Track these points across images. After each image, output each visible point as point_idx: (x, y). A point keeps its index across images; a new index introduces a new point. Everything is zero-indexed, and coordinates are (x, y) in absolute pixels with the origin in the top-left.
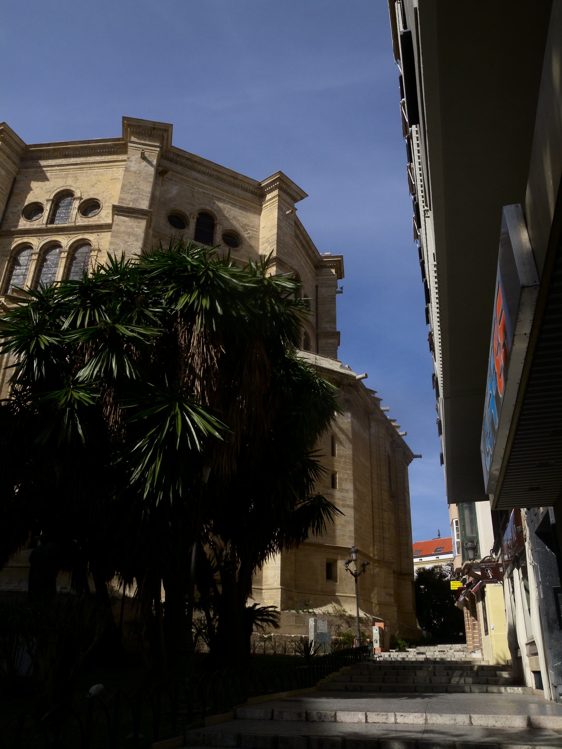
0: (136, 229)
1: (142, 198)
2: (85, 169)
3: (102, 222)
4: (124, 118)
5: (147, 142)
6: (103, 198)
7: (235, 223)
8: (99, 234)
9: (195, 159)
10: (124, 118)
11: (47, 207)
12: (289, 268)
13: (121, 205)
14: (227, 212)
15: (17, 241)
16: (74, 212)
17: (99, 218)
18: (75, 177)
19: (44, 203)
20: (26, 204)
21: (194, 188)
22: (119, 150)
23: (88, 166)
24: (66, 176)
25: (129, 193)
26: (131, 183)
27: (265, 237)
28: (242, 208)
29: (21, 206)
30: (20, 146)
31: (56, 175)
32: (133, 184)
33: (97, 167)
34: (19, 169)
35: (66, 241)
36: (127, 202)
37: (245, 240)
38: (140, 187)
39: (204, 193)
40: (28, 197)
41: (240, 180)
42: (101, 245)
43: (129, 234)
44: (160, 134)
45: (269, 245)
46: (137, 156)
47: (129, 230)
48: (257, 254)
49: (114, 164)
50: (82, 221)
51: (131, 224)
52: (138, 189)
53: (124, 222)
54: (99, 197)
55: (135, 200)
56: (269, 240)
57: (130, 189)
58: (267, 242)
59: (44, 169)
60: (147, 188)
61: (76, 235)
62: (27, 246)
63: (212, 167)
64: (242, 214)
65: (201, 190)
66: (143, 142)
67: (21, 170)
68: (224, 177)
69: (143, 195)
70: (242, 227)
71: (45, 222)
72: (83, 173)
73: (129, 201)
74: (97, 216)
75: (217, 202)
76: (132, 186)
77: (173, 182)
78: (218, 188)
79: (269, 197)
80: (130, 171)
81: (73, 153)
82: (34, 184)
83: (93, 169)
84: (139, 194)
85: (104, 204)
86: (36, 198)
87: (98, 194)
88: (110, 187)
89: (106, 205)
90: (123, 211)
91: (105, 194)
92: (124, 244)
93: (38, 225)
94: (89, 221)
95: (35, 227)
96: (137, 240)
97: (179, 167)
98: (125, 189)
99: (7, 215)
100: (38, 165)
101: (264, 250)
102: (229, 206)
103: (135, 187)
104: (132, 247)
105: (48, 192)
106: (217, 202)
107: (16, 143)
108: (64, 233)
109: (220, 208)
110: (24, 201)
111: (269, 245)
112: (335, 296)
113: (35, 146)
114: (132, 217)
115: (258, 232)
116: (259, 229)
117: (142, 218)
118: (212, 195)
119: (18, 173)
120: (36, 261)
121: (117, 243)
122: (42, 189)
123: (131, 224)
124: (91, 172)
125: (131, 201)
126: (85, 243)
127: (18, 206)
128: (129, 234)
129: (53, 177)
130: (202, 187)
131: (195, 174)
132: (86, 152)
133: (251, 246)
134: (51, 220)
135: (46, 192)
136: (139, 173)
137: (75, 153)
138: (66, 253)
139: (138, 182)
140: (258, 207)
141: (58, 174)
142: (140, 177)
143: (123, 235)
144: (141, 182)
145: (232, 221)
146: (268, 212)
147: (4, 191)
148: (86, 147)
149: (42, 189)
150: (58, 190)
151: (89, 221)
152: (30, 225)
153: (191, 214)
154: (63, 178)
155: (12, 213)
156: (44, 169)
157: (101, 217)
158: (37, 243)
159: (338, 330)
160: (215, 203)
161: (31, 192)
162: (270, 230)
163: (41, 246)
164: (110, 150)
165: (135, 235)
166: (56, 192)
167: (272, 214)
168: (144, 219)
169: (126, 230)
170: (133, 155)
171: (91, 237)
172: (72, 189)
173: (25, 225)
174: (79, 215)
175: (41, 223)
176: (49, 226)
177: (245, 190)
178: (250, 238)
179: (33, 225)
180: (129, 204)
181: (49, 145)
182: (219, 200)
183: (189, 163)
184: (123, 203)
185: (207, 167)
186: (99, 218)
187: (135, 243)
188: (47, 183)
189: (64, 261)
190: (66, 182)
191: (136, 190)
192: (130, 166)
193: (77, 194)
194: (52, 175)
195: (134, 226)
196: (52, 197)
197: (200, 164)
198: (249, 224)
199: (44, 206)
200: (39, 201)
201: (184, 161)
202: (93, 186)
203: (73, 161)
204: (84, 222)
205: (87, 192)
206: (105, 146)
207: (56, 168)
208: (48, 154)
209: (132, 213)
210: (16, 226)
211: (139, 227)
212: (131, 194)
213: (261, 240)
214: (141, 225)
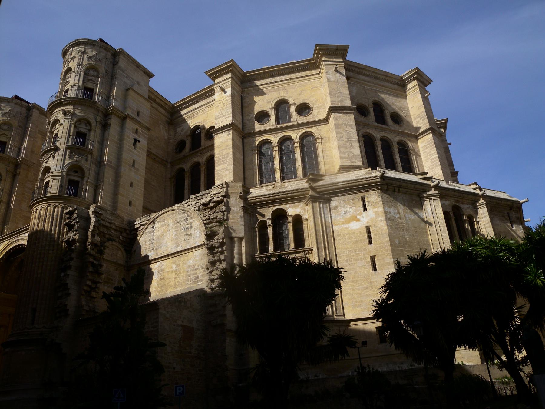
0: (349, 121)
1: (345, 99)
2: (290, 83)
4: (349, 45)
5: (334, 60)
7: (394, 107)
8: (317, 127)
9: (361, 67)
10: (349, 45)
11: (272, 113)
12: (438, 133)
13: (333, 105)
14: (388, 100)
15: (258, 140)
16: (294, 114)
17: (313, 116)
18: (285, 90)
19: (269, 110)
20: (255, 113)
21: (365, 87)
22: (311, 67)
23: (292, 81)
25: (336, 96)
26: (334, 89)
27: (415, 114)
28: (395, 96)
29: (252, 114)
30: (241, 74)
31: (270, 90)
32: (336, 90)
33: (298, 81)
34: (242, 89)
35: (295, 135)
36: (337, 103)
37: (404, 118)
38: (341, 91)
39: (371, 89)
40: (255, 107)
41: (390, 77)
42: (322, 135)
43: (346, 125)
44: (342, 53)
45: (420, 119)
46: (332, 70)
47: (345, 122)
48: (413, 127)
49: (310, 77)
50: (301, 120)
51: (345, 118)
52: (341, 93)
53: (340, 117)
55: (341, 101)
56: (420, 116)
57: (335, 94)
58: (418, 118)
59: (260, 87)
60: (345, 91)
61: (301, 130)
62: (267, 142)
63: (372, 70)
64: (396, 100)
65: (369, 88)
66: (332, 60)
67: (243, 90)
68: (379, 76)
69: (345, 97)
70: (399, 109)
71: (274, 123)
72: (289, 86)
73: (337, 102)
74: (311, 115)
75: (380, 94)
76: (336, 91)
77: (351, 85)
78: (378, 84)
79: (409, 86)
80: (331, 81)
81: (278, 73)
82: (256, 98)
83: (296, 82)
84: (342, 96)
85: (314, 106)
86: (262, 108)
87: (307, 99)
88: (313, 93)
90: (337, 110)
92: (345, 132)
94: (306, 119)
95: (268, 128)
96: (352, 128)
97: (352, 73)
98: (332, 94)
99: (244, 122)
100: (255, 85)
101: (418, 123)
102: (387, 96)
103: (338, 92)
104: (351, 133)
105: (268, 103)
106: (380, 94)
107: (239, 71)
108: (292, 129)
109: (383, 98)
110: (253, 111)
111: (420, 119)
112: (448, 147)
113: (250, 72)
114: (343, 113)
115: (409, 111)
116: (409, 109)
117: (350, 113)
118: (376, 90)
119: (242, 92)
120: (278, 151)
121: (341, 132)
122: (264, 101)
123: (345, 118)
124: (295, 85)
125: (339, 102)
127: (250, 115)
128: (346, 125)
130: (369, 86)
131: (362, 77)
132: (287, 71)
133: (408, 122)
134: (278, 122)
135: (267, 103)
136: (337, 82)
137: (279, 73)
138: (298, 143)
139: (339, 88)
140: (404, 94)
141: (272, 89)
142: (338, 84)
143: (342, 126)
144: (341, 88)
145: (392, 106)
146: (412, 97)
148: (287, 68)
149: (264, 101)
151: (306, 119)
152: (264, 127)
153: (369, 105)
154: (275, 91)
155: (248, 120)
156: (260, 87)
157: (315, 115)
158: (274, 139)
159: (456, 170)
160: (379, 95)
161: (256, 104)
162: (418, 109)
163: (277, 140)
164: (304, 68)
165: (350, 125)
167: (417, 97)
168: (352, 113)
169: (344, 123)
170: (329, 70)
171: (313, 130)
173: (260, 128)
174: (298, 115)
175: (272, 125)
176: (279, 126)
177: (393, 83)
178: (406, 116)
179: (266, 127)
180: (338, 104)
181: (260, 70)
182: (381, 92)
183: (357, 70)
184: (334, 104)
185: (369, 71)
186: (313, 116)
187: (352, 130)
188: (265, 96)
189: (298, 148)
190: (279, 94)
191: (340, 94)
192: (330, 78)
193: (291, 101)
194: (267, 90)
195: (347, 119)
196: (273, 106)
197: (364, 69)
198: (402, 106)
199: (270, 113)
200: (265, 109)
201: (354, 69)
202: (300, 94)
203: (279, 79)
204: (304, 120)
205: (297, 99)
206: (300, 66)
207: (269, 85)
208: (260, 76)
209: (343, 110)
210: (254, 129)
211: (351, 119)
212: (338, 97)
213: (412, 117)
214: (351, 117)
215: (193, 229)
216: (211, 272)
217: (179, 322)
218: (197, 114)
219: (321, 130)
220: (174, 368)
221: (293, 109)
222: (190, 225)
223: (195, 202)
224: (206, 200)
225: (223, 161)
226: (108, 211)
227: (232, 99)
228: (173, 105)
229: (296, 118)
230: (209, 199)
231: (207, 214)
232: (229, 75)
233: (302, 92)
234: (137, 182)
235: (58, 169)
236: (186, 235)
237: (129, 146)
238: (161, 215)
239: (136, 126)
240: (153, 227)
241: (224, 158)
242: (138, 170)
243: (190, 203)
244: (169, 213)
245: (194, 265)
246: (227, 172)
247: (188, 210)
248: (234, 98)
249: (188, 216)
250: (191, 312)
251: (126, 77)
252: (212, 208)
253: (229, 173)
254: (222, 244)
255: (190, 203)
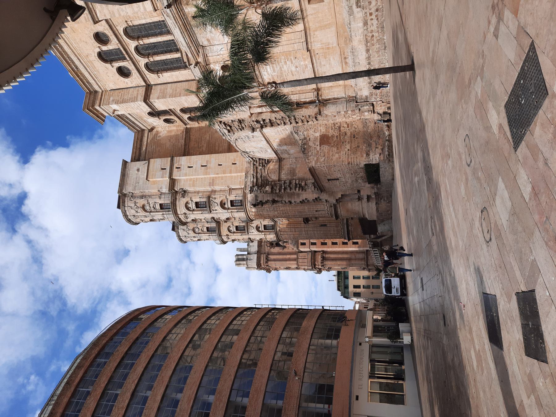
3: (107, 26)
6: (90, 32)
11: (117, 65)
23: (75, 51)
24: (90, 62)
35: (132, 45)
54: (92, 35)
71: (127, 63)
72: (82, 53)
83: (74, 47)
87: (89, 37)
89: (94, 29)
91: (87, 33)
93: (131, 66)
94: (111, 36)
122: (107, 73)
126: (126, 31)
129: (95, 69)
134: (124, 59)
147: (122, 93)
149: (107, 73)
150: (102, 63)
152: (133, 70)
155: (132, 83)
166: (104, 64)
169: (105, 8)
172: (96, 55)
173: (135, 73)
179: (132, 68)
186: (105, 30)
190: (95, 60)
193: (98, 50)
200: (116, 71)
202: (86, 42)
203: (78, 62)
204: (113, 38)
207: (89, 70)
215: (249, 135)
216: (279, 125)
217: (318, 148)
218: (137, 116)
219: (118, 22)
220: (348, 150)
221: (105, 48)
222: (246, 137)
223: (228, 136)
224: (226, 132)
225: (180, 103)
226: (246, 180)
227: (120, 103)
228: (135, 133)
229: (113, 45)
230: (224, 130)
231: (236, 130)
232: (97, 107)
233: (83, 41)
234: (217, 160)
235: (227, 215)
236: (253, 138)
237: (192, 172)
238: (240, 150)
239: (175, 170)
240: (250, 152)
241: (177, 102)
242: (207, 162)
243: (229, 138)
244: (238, 147)
245: (274, 132)
246: (189, 99)
247: (235, 139)
248: (118, 101)
249: (239, 138)
250: (310, 139)
251: (138, 183)
252: (230, 127)
253: (189, 98)
254: (257, 122)
255: (229, 138)
